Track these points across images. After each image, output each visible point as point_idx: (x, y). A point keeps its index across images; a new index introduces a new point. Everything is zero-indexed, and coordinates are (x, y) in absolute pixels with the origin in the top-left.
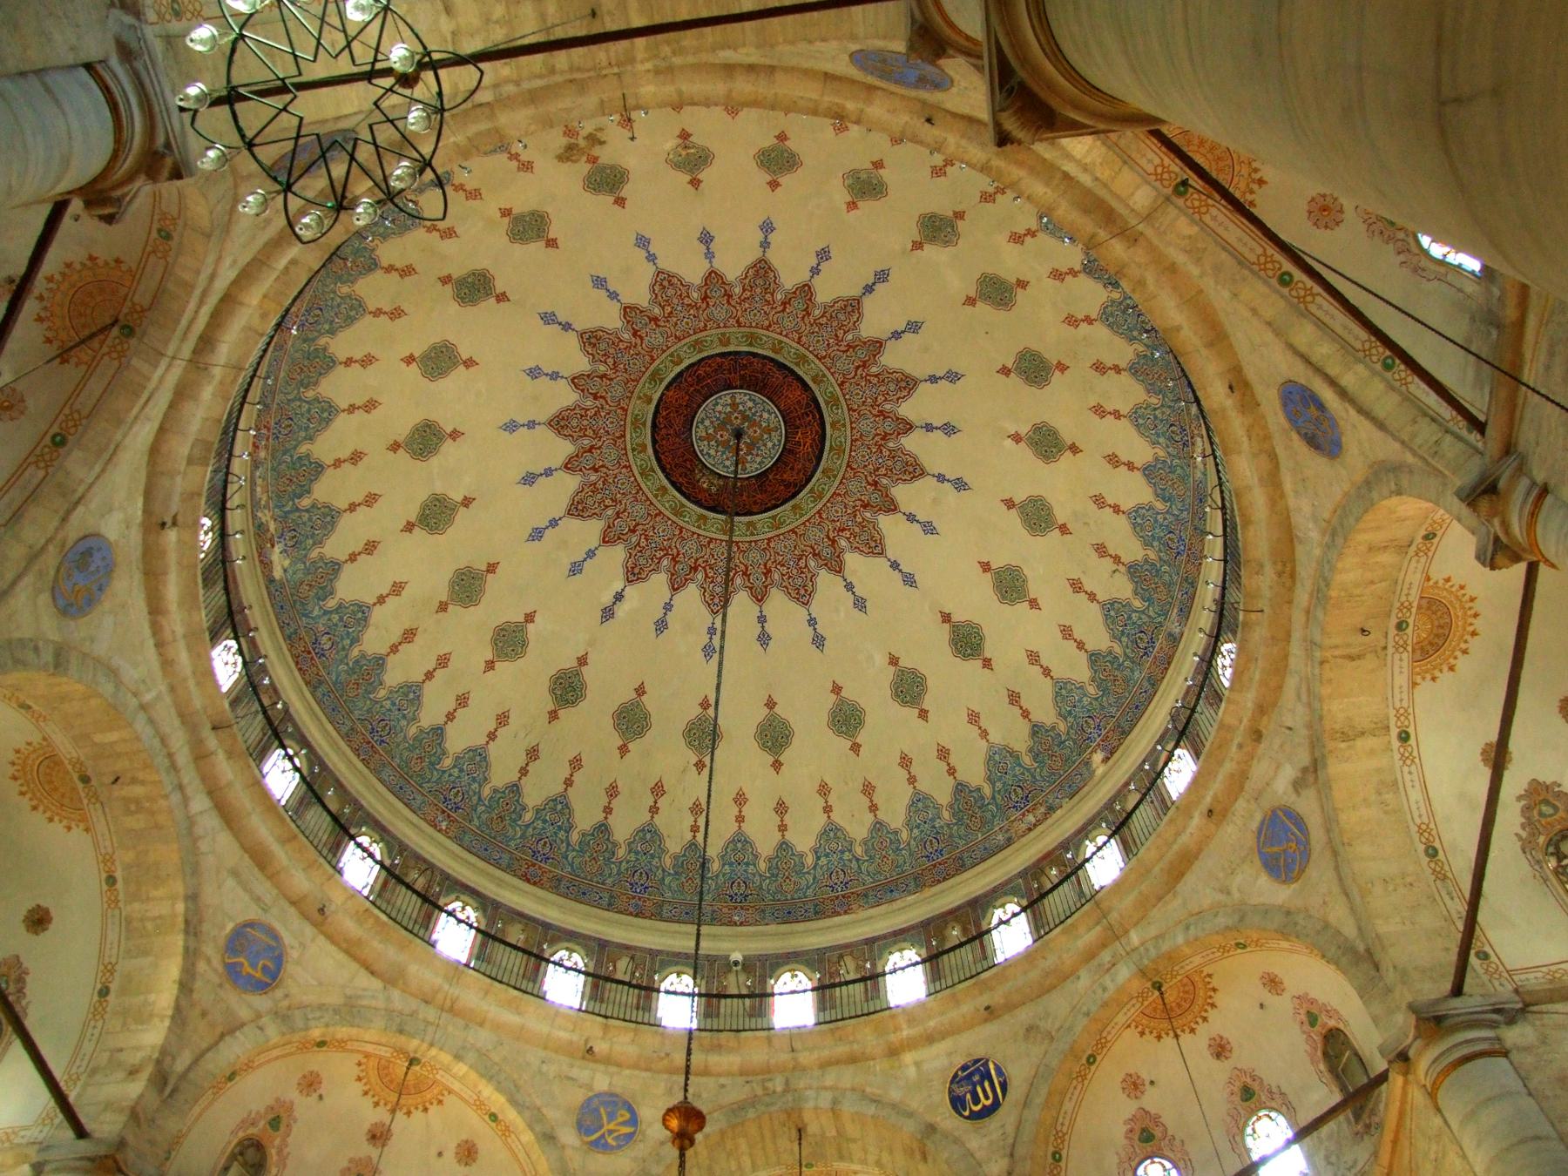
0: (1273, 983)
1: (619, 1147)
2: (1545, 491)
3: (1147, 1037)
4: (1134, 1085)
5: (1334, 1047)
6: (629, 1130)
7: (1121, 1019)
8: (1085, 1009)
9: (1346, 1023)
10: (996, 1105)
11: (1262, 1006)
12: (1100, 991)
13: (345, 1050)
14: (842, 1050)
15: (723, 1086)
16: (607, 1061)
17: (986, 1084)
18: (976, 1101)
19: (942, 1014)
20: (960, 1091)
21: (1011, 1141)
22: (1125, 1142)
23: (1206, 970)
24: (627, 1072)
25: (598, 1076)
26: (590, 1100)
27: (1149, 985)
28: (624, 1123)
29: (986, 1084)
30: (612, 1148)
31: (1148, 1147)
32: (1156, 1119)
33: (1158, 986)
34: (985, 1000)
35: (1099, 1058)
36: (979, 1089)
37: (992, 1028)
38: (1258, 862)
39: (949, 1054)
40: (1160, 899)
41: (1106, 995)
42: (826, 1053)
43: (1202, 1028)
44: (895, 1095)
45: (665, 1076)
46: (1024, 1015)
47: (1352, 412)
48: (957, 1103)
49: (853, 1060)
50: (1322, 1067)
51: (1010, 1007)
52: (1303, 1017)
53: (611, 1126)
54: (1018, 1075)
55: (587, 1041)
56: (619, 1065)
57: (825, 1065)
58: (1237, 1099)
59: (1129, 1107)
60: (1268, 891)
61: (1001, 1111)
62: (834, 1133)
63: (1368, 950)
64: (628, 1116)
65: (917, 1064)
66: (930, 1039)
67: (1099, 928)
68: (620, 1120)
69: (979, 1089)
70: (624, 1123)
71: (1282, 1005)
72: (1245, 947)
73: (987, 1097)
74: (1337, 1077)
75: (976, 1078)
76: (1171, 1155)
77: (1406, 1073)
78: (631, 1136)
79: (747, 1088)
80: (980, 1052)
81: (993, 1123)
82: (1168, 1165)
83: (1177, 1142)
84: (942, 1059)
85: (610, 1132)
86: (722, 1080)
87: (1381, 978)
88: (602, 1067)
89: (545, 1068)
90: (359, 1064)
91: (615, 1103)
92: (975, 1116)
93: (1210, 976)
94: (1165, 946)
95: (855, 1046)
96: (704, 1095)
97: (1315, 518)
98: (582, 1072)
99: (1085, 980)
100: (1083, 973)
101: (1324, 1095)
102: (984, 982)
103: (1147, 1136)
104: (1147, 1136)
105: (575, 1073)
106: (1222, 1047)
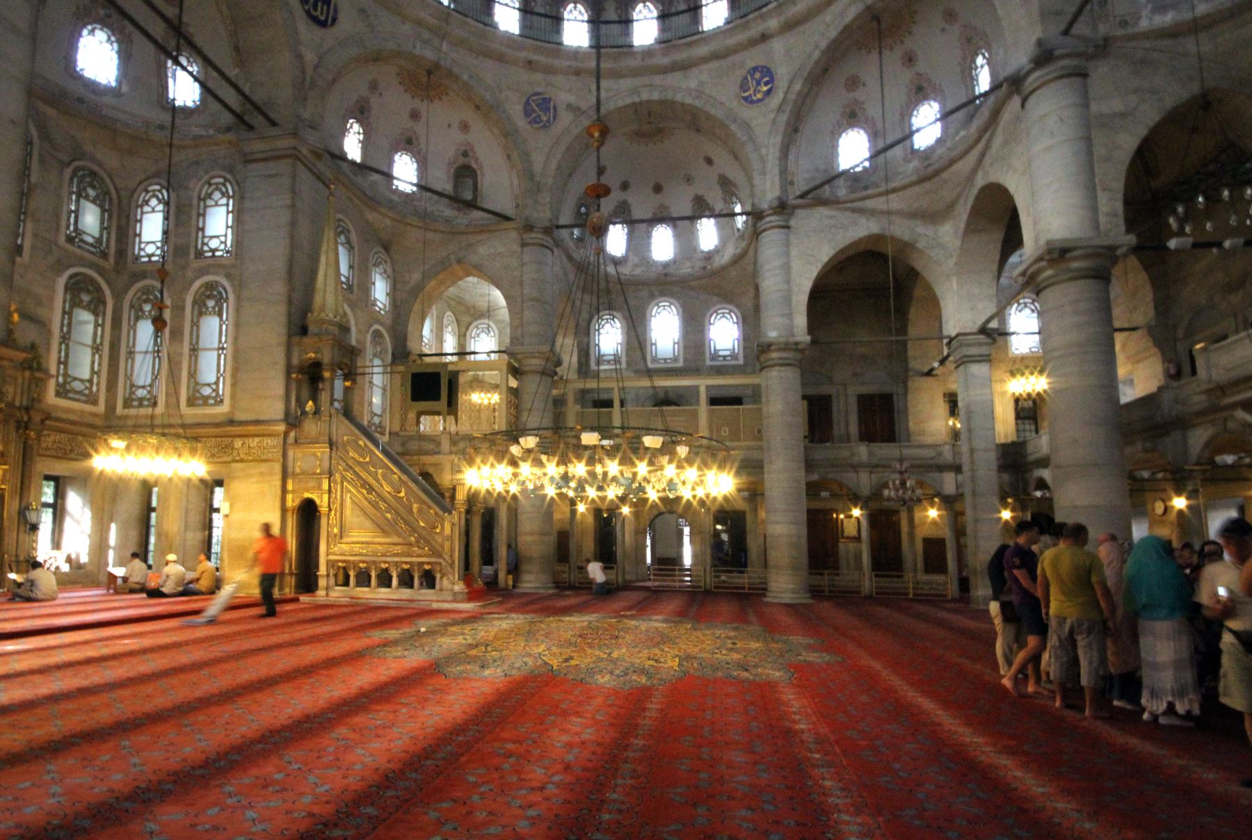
0: (465, 127)
2: (788, 227)
4: (374, 86)
5: (465, 172)
7: (402, 62)
18: (316, 9)
38: (524, 100)
40: (471, 50)
43: (417, 101)
47: (772, 116)
52: (463, 148)
60: (516, 111)
67: (436, 22)
71: (458, 137)
81: (320, 32)
92: (308, 12)
94: (456, 70)
97: (701, 84)
99: (407, 28)
103: (362, 112)
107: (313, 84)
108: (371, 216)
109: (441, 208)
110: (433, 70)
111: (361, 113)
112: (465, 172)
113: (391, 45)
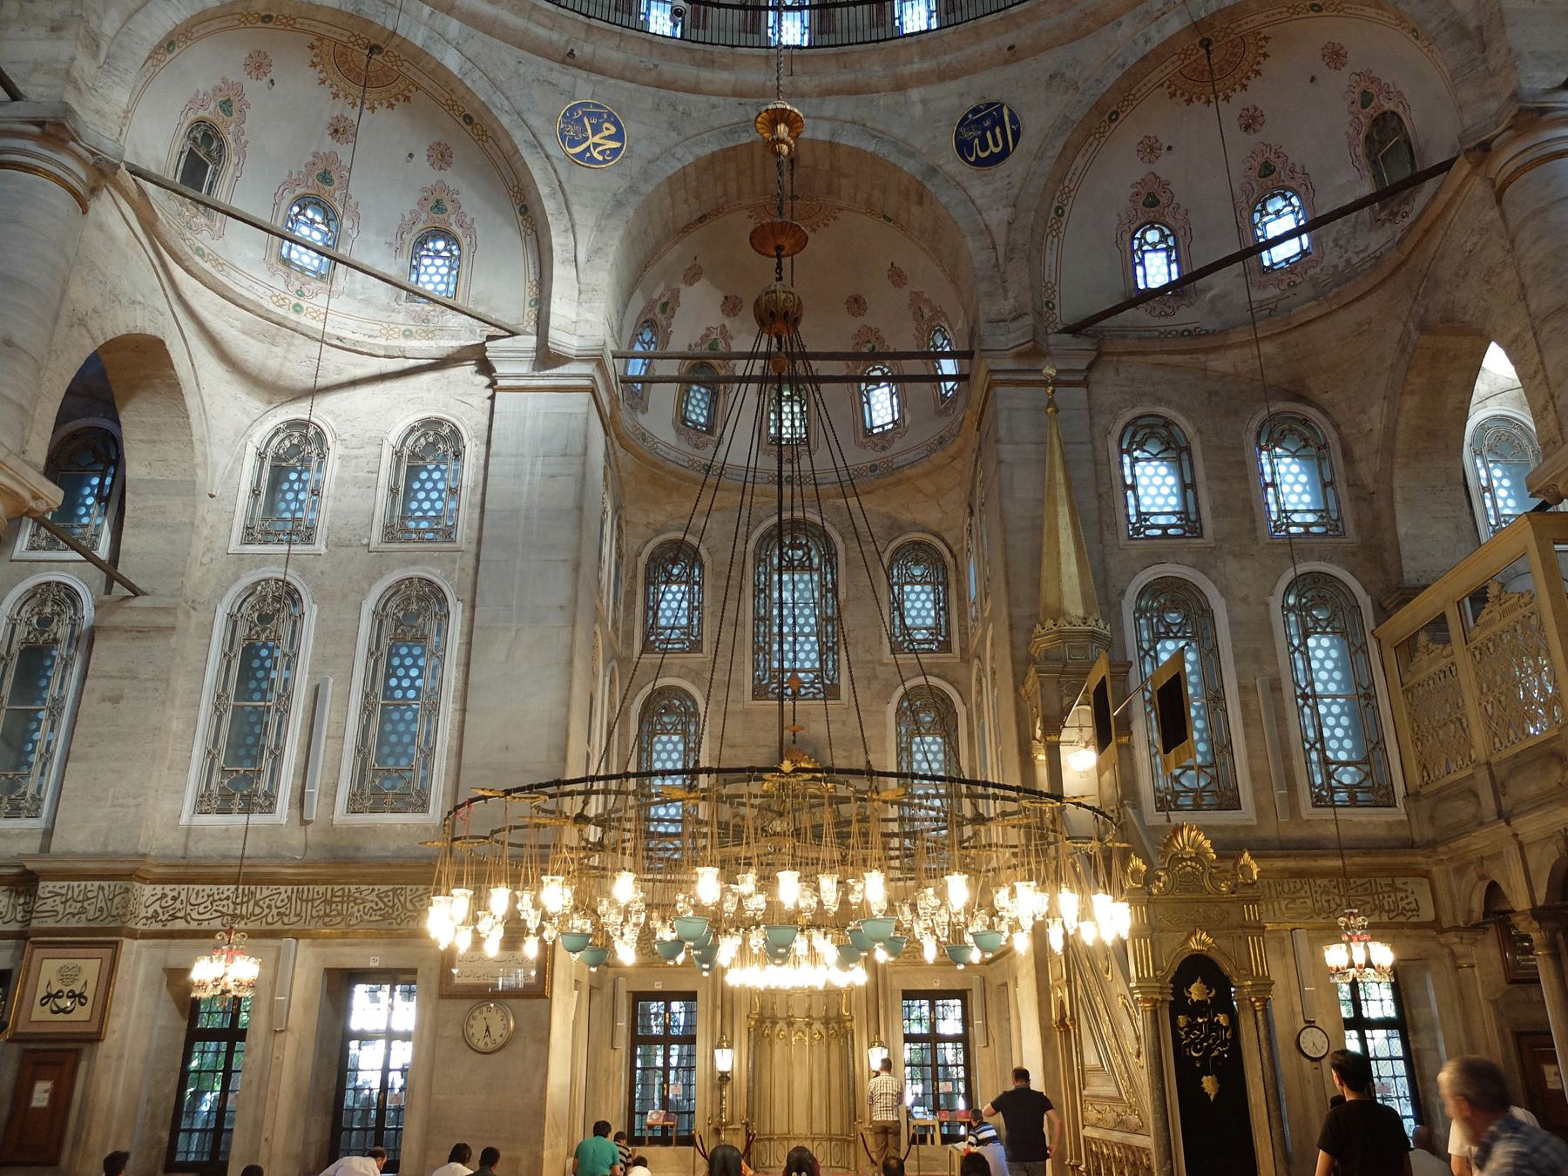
0: (1335, 56)
1: (605, 161)
3: (1178, 98)
4: (1150, 149)
5: (1384, 135)
6: (618, 145)
7: (1156, 76)
8: (1120, 60)
9: (1407, 107)
10: (1005, 153)
11: (1313, 79)
12: (1141, 42)
13: (294, 29)
14: (846, 77)
15: (714, 106)
16: (589, 67)
17: (998, 130)
18: (984, 147)
19: (960, 49)
20: (967, 135)
21: (1015, 191)
22: (1129, 204)
23: (1265, 32)
24: (612, 81)
25: (580, 82)
26: (572, 109)
27: (1197, 41)
28: (609, 138)
29: (998, 130)
30: (599, 162)
31: (1152, 213)
32: (1165, 186)
33: (1206, 44)
34: (1008, 38)
35: (1122, 116)
36: (989, 134)
37: (1012, 71)
39: (961, 95)
41: (1148, 48)
42: (827, 80)
43: (1239, 98)
44: (898, 131)
45: (653, 90)
46: (1049, 61)
48: (963, 147)
49: (855, 90)
50: (1359, 151)
51: (1037, 49)
52: (1357, 97)
53: (597, 139)
54: (1033, 126)
55: (568, 42)
56: (601, 73)
57: (827, 92)
58: (1253, 174)
59: (1140, 170)
61: (1010, 158)
62: (827, 166)
63: (1479, 28)
64: (613, 130)
65: (924, 102)
66: (942, 76)
68: (606, 133)
69: (989, 134)
70: (609, 138)
72: (1321, 9)
73: (996, 145)
74: (1374, 163)
75: (987, 123)
76: (1172, 222)
77: (1476, 166)
78: (615, 152)
79: (741, 110)
80: (993, 99)
82: (1167, 232)
83: (1181, 211)
84: (954, 99)
85: (596, 145)
86: (713, 99)
87: (1485, 61)
88: (584, 74)
89: (522, 69)
90: (312, 47)
91: (600, 115)
92: (980, 163)
93: (1266, 39)
95: (860, 75)
96: (694, 114)
98: (563, 77)
99: (1126, 28)
100: (1126, 20)
101: (1351, 181)
102: (1013, 17)
103: (1152, 201)
104: (1152, 201)
105: (555, 77)
106: (1253, 118)
107: (1011, 248)
108: (1220, 363)
109: (1361, 244)
110: (1203, 33)
111: (1153, 206)
112: (1384, 135)
113: (1115, 74)
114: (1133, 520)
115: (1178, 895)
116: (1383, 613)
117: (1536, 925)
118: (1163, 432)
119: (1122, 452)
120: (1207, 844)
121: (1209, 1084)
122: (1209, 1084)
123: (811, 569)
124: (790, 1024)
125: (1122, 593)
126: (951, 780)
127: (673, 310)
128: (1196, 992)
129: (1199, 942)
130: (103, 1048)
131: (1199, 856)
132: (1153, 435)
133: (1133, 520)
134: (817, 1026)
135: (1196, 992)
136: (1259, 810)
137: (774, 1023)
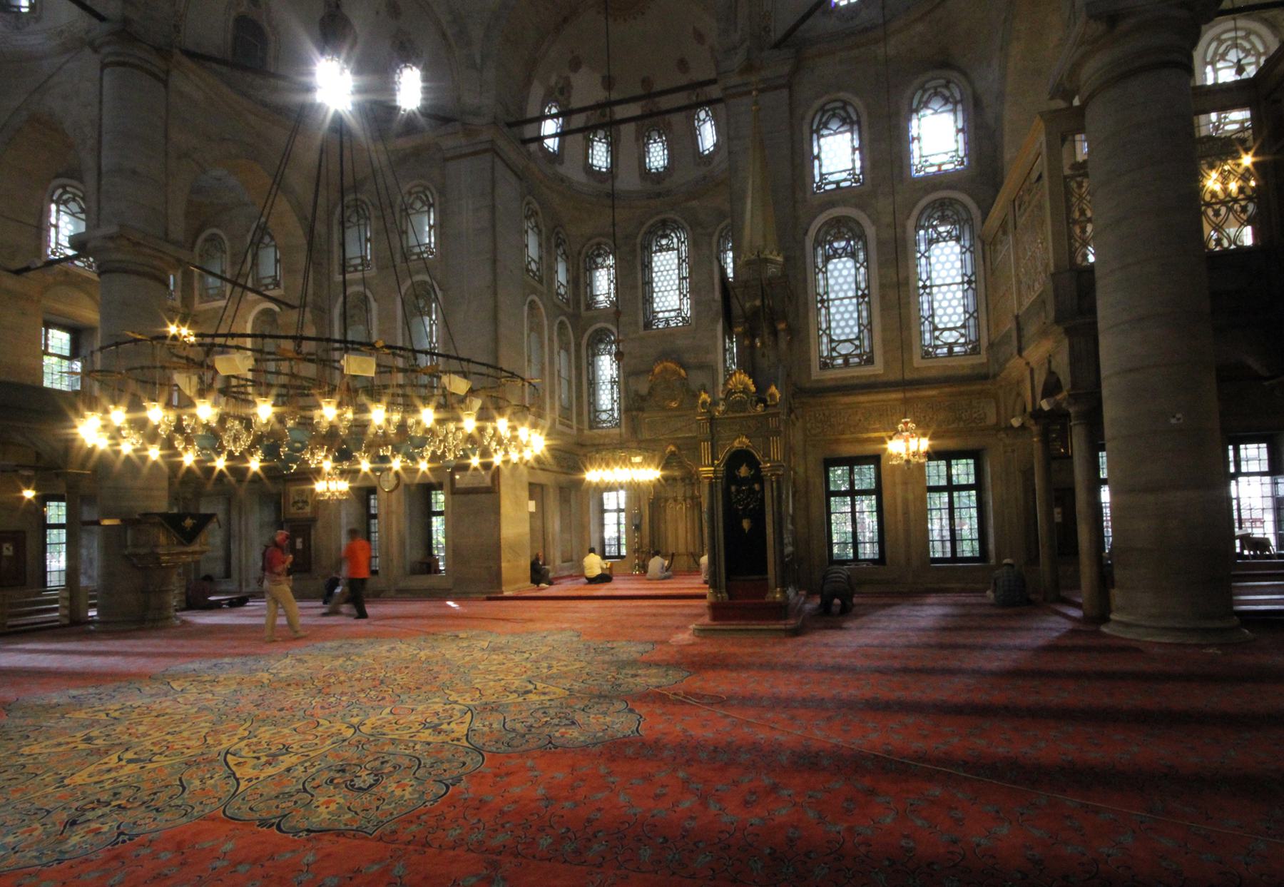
114: (817, 179)
115: (731, 415)
116: (985, 215)
117: (1032, 422)
118: (842, 113)
119: (812, 132)
120: (750, 382)
121: (746, 524)
122: (746, 524)
123: (673, 249)
124: (675, 500)
125: (806, 233)
126: (448, 357)
127: (569, 92)
128: (744, 471)
129: (741, 442)
130: (319, 524)
131: (745, 390)
132: (834, 115)
133: (817, 179)
134: (689, 501)
135: (744, 471)
136: (886, 363)
137: (666, 500)
